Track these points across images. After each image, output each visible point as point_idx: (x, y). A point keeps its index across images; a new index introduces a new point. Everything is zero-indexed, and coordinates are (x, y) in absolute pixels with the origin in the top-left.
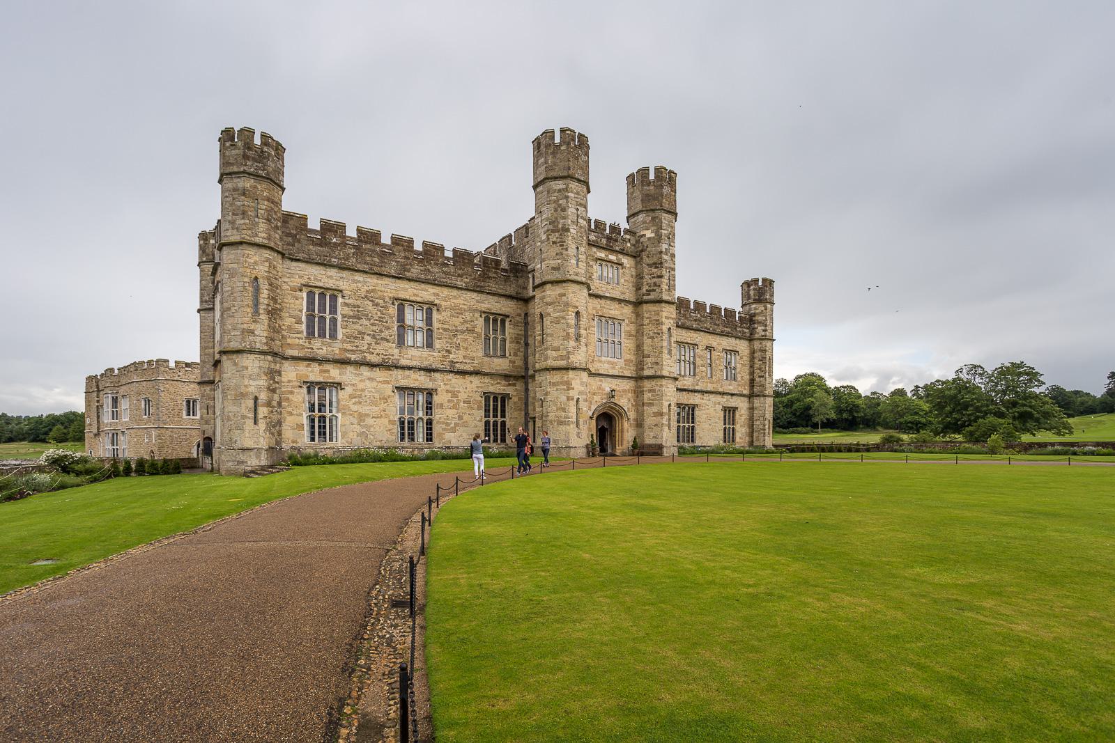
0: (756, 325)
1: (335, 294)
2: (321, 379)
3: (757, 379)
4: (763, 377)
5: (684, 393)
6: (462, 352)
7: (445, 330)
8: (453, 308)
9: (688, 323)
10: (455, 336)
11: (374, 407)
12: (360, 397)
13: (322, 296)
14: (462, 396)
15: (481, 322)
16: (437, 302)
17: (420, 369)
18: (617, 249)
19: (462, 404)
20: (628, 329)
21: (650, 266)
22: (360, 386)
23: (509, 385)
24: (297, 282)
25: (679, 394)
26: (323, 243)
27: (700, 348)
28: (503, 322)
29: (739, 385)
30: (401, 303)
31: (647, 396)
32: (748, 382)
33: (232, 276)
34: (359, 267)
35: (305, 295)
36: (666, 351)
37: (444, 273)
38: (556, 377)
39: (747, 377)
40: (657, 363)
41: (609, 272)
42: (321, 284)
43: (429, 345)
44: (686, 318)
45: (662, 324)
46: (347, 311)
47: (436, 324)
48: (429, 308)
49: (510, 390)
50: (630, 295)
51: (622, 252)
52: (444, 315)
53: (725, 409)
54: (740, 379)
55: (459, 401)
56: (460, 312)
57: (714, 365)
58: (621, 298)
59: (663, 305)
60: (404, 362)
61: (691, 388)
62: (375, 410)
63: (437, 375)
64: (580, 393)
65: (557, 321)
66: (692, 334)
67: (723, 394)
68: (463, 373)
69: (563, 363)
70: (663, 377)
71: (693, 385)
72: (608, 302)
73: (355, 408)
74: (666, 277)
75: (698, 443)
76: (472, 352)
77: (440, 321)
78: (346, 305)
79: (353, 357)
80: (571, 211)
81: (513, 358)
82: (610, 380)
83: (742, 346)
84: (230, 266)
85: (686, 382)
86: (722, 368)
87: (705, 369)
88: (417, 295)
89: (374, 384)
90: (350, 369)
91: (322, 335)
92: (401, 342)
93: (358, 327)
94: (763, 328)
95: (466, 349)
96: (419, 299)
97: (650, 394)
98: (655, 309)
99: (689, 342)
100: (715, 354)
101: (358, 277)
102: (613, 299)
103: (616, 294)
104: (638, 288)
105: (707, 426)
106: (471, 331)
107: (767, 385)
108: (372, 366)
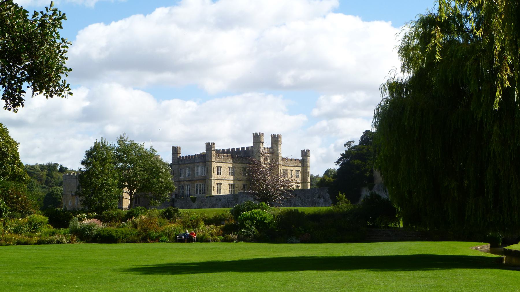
0: (305, 163)
1: (221, 167)
7: (237, 172)
9: (286, 165)
13: (219, 168)
22: (224, 184)
26: (219, 158)
35: (217, 168)
42: (219, 166)
47: (235, 171)
49: (247, 184)
52: (236, 169)
56: (238, 168)
73: (223, 188)
78: (222, 169)
79: (223, 179)
91: (219, 175)
92: (230, 175)
108: (226, 180)
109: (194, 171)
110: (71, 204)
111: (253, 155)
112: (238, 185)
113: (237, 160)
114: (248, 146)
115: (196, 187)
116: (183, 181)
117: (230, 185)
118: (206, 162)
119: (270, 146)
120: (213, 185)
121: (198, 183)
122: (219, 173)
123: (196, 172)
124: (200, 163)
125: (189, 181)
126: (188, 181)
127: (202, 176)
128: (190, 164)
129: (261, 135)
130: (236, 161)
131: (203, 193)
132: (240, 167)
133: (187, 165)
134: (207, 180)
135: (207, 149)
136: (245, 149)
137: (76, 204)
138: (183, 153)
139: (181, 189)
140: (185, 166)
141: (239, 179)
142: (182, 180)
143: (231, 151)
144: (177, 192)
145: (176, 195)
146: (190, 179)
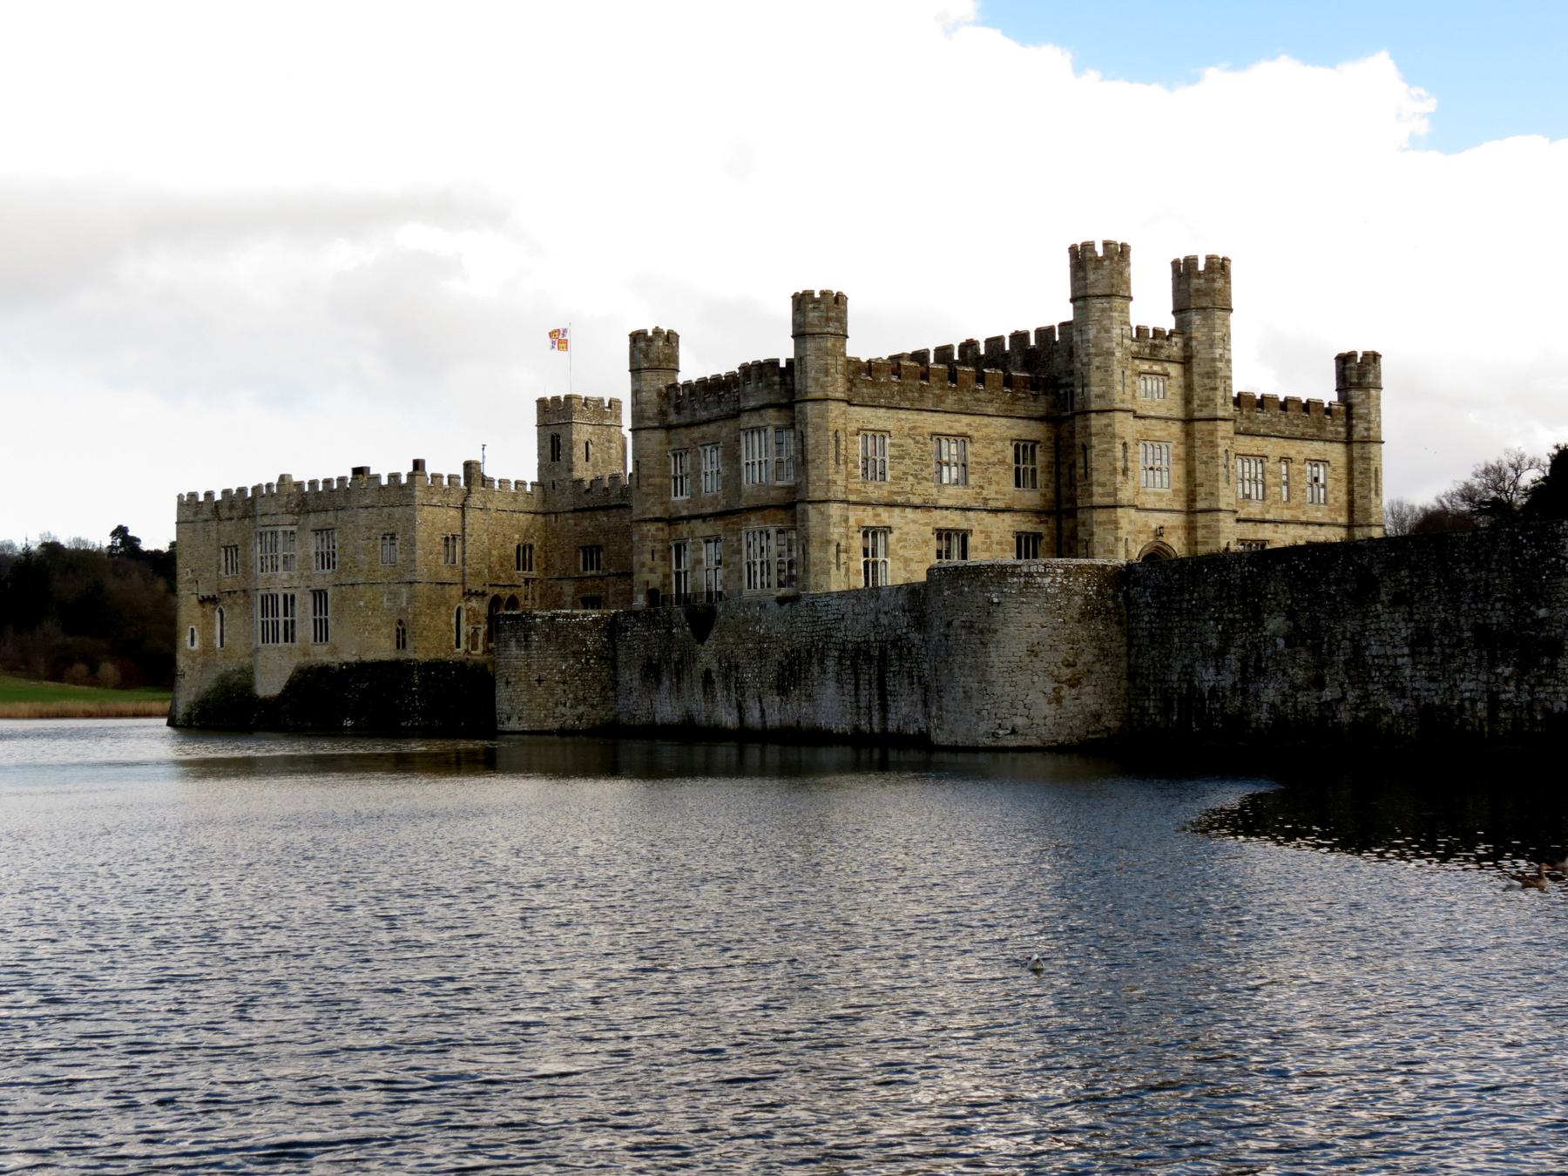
2: (873, 524)
3: (1358, 502)
4: (1365, 497)
5: (1250, 524)
6: (994, 487)
7: (978, 463)
8: (986, 437)
9: (1254, 428)
10: (987, 469)
11: (918, 553)
12: (905, 540)
14: (995, 537)
15: (1010, 452)
16: (969, 433)
17: (956, 509)
18: (1163, 357)
19: (994, 546)
20: (1176, 451)
21: (1202, 375)
22: (906, 529)
23: (1041, 522)
24: (853, 427)
25: (1242, 526)
26: (875, 384)
27: (1271, 460)
28: (1033, 449)
29: (1331, 510)
30: (937, 436)
31: (1200, 533)
32: (1345, 505)
33: (817, 428)
34: (903, 405)
35: (860, 438)
36: (1222, 478)
37: (976, 399)
38: (1100, 516)
39: (1343, 498)
40: (1212, 494)
41: (1152, 384)
42: (871, 427)
43: (966, 483)
44: (1251, 421)
45: (1217, 446)
46: (894, 451)
47: (970, 459)
48: (964, 438)
49: (1042, 529)
50: (1178, 412)
51: (1169, 360)
55: (992, 543)
56: (990, 441)
57: (1292, 483)
58: (1168, 415)
59: (1219, 422)
60: (942, 502)
61: (1259, 517)
62: (917, 554)
63: (971, 514)
64: (1128, 533)
65: (1104, 453)
66: (1258, 441)
67: (1307, 524)
68: (996, 511)
69: (1109, 501)
70: (1220, 510)
71: (1262, 513)
72: (1154, 421)
74: (1221, 389)
76: (1003, 488)
77: (973, 454)
78: (892, 445)
79: (900, 499)
80: (1116, 332)
81: (1043, 490)
82: (1157, 515)
84: (815, 420)
85: (1251, 510)
86: (1303, 487)
87: (1278, 489)
88: (951, 428)
89: (917, 526)
90: (897, 511)
93: (902, 467)
94: (1366, 425)
95: (998, 483)
96: (953, 432)
97: (1204, 531)
98: (1209, 427)
100: (1294, 467)
101: (902, 414)
103: (1163, 412)
104: (1187, 400)
106: (1002, 462)
107: (1373, 510)
108: (917, 507)
109: (738, 459)
110: (196, 643)
111: (1071, 373)
112: (988, 537)
113: (982, 395)
114: (1045, 324)
115: (745, 547)
116: (689, 518)
117: (939, 538)
118: (797, 407)
119: (1168, 323)
120: (836, 533)
121: (755, 523)
122: (873, 469)
123: (744, 461)
124: (763, 412)
125: (717, 516)
126: (711, 515)
127: (779, 483)
128: (721, 423)
129: (1118, 254)
130: (979, 400)
131: (780, 585)
132: (1003, 439)
133: (705, 428)
134: (799, 507)
135: (800, 335)
136: (1032, 342)
137: (218, 645)
138: (691, 369)
139: (679, 565)
140: (696, 433)
141: (992, 504)
142: (685, 513)
143: (956, 357)
144: (655, 580)
145: (652, 595)
146: (719, 508)
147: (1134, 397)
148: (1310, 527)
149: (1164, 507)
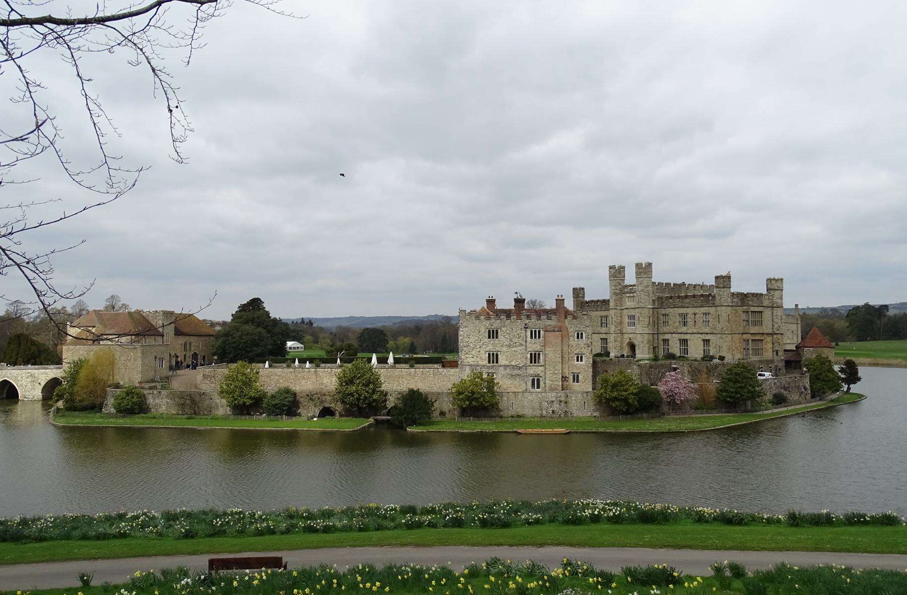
9: (684, 305)
26: (588, 306)
30: (601, 317)
48: (606, 317)
53: (704, 340)
54: (711, 326)
60: (602, 332)
61: (685, 332)
66: (685, 309)
67: (702, 334)
71: (686, 330)
72: (631, 309)
75: (689, 355)
83: (712, 310)
85: (683, 330)
87: (692, 323)
99: (684, 312)
100: (697, 316)
102: (632, 308)
105: (693, 348)
129: (622, 268)
147: (625, 303)
148: (703, 335)
149: (633, 332)
